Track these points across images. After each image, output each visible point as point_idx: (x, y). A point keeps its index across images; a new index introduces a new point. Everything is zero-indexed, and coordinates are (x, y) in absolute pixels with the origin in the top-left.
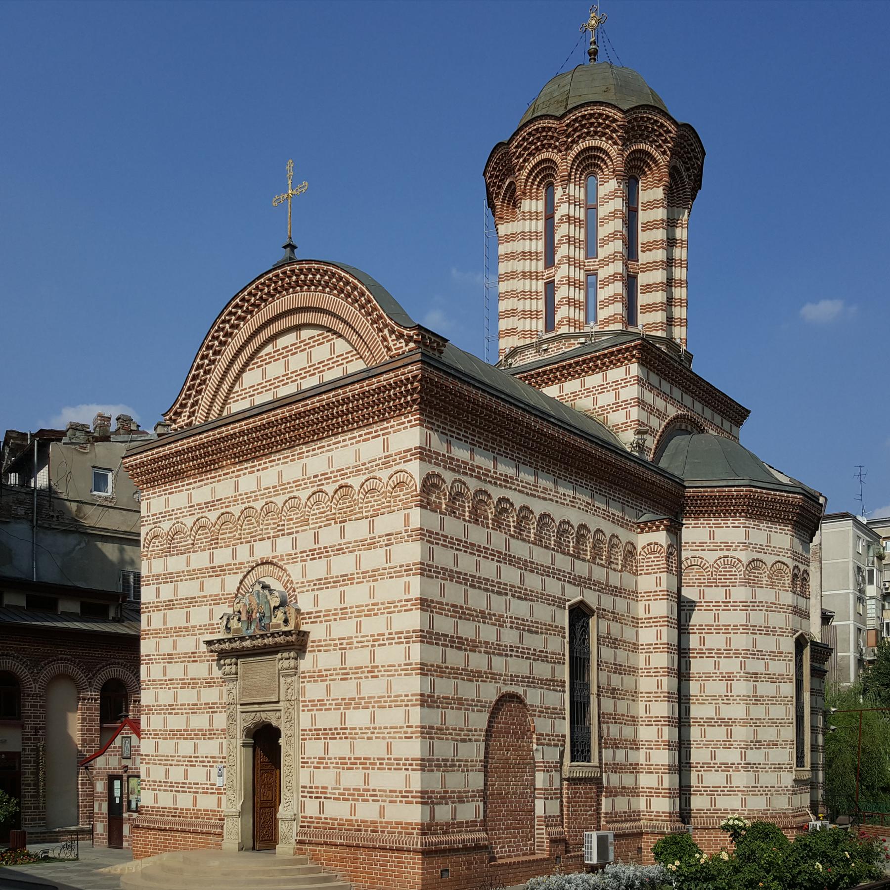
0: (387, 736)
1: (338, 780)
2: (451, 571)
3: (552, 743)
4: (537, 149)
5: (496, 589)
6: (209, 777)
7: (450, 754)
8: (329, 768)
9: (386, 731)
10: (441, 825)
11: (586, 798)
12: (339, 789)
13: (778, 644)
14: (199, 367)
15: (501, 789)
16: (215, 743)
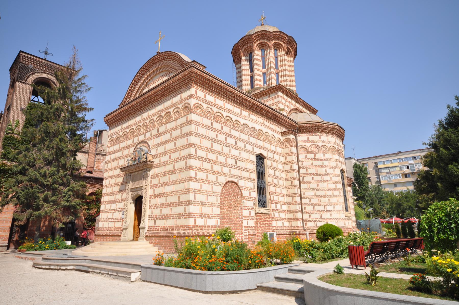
0: (178, 194)
1: (161, 212)
2: (206, 136)
3: (250, 200)
4: (246, 44)
5: (225, 145)
6: (120, 216)
7: (204, 200)
8: (158, 208)
9: (178, 192)
10: (200, 226)
11: (265, 220)
12: (161, 215)
13: (334, 171)
14: (130, 90)
15: (228, 215)
16: (122, 204)
